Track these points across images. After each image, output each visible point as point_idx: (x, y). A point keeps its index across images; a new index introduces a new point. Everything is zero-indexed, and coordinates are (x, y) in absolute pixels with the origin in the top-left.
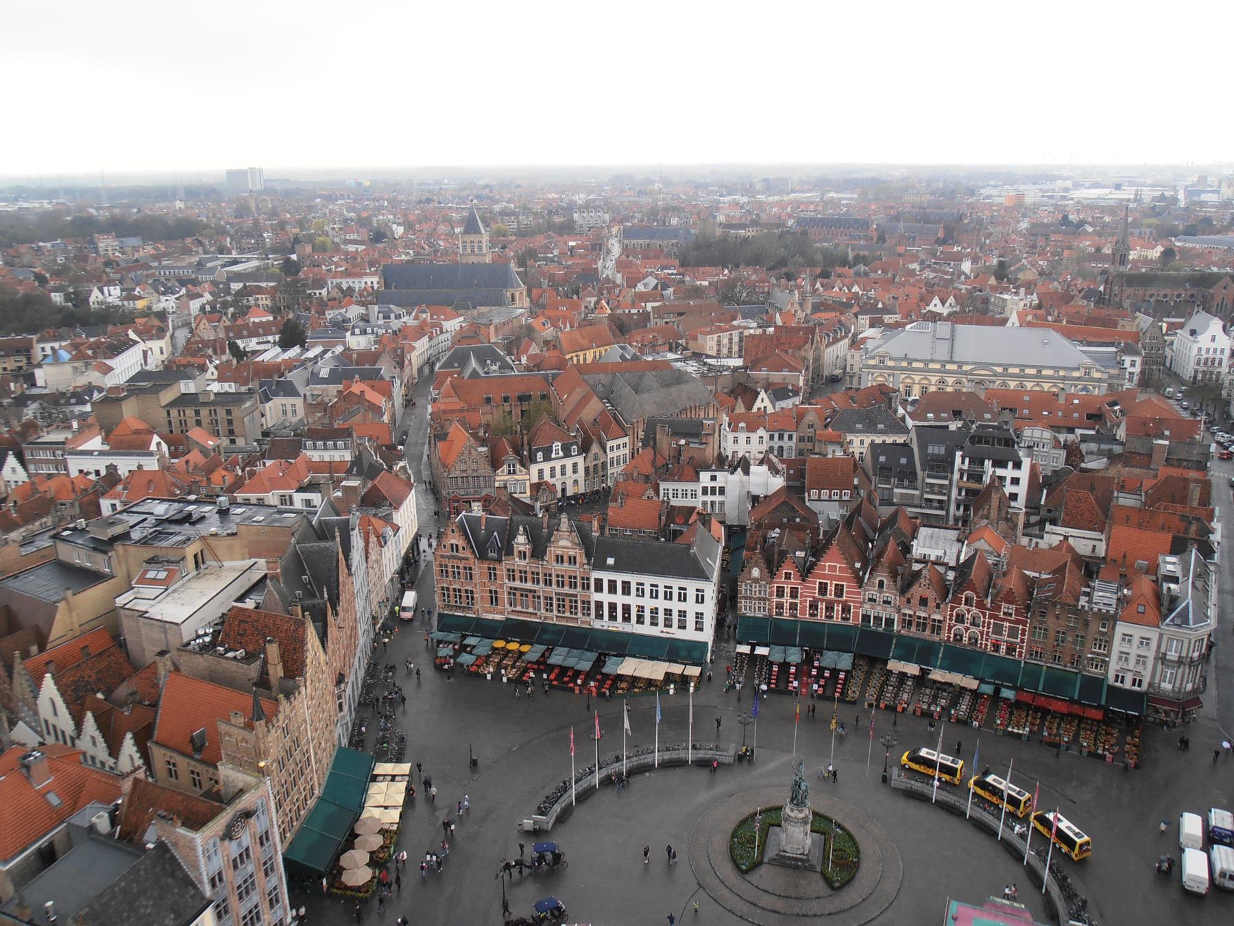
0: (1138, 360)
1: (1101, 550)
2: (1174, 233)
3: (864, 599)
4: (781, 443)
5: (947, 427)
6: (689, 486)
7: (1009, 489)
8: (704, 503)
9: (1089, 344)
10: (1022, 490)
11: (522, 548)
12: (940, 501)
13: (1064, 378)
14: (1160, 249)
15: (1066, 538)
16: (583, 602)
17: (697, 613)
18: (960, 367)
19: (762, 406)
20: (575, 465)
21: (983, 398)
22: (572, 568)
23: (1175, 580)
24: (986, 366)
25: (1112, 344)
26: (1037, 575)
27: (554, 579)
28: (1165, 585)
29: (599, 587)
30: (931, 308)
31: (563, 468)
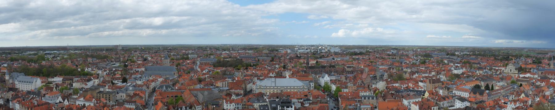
4: (238, 106)
19: (233, 98)
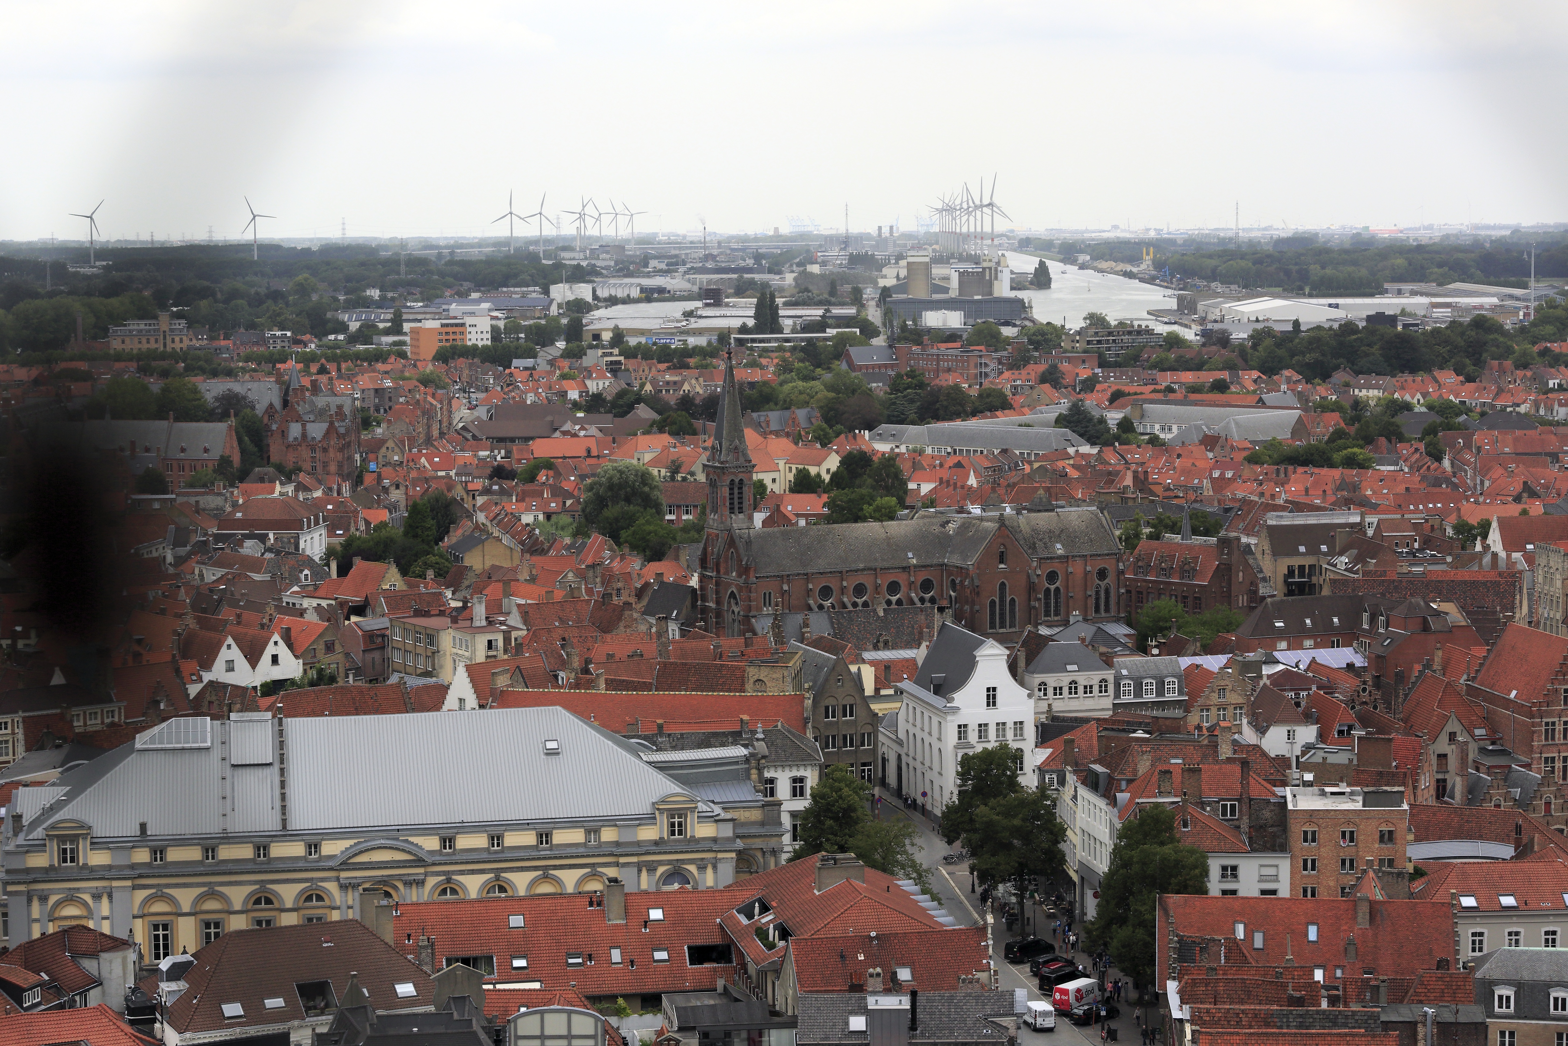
0: (811, 778)
9: (679, 743)
13: (617, 851)
18: (313, 847)
21: (389, 938)
25: (735, 738)
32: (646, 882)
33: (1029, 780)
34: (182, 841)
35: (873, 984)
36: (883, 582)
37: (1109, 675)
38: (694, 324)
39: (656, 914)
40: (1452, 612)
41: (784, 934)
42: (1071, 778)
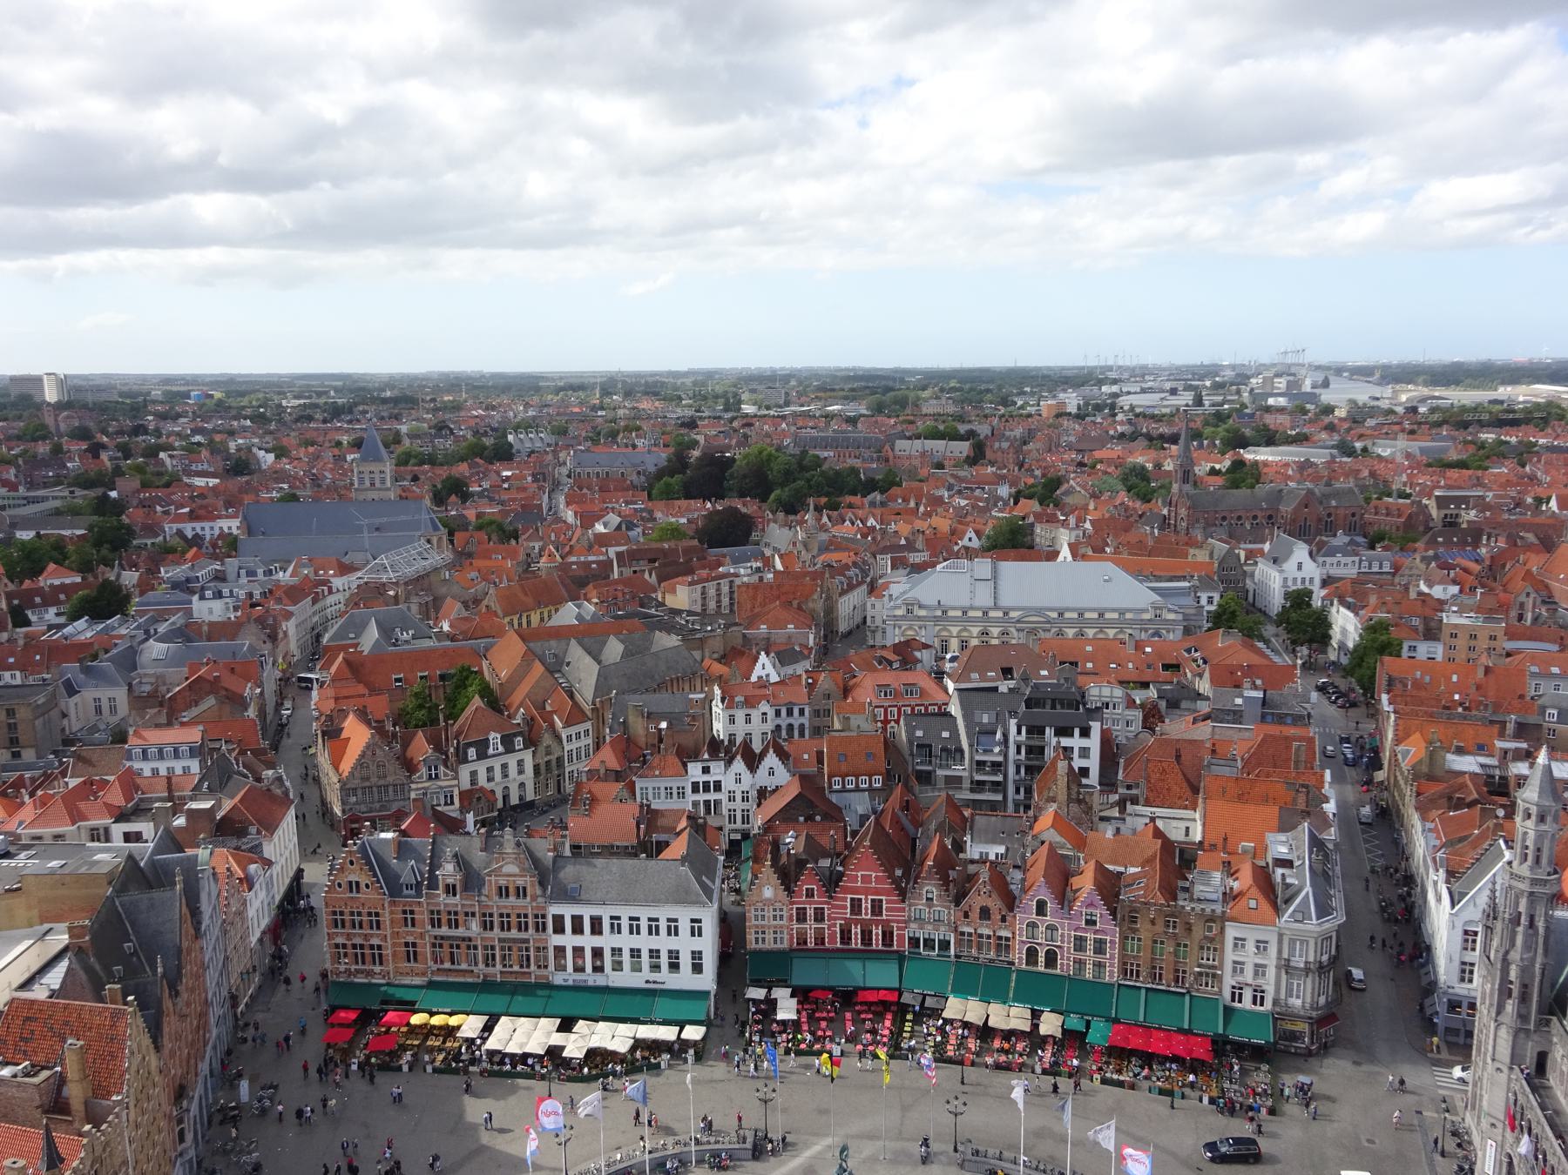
1: (1197, 835)
2: (1244, 443)
3: (909, 916)
4: (790, 720)
5: (996, 689)
6: (674, 783)
7: (1078, 763)
8: (695, 804)
9: (1159, 579)
10: (1093, 763)
11: (450, 881)
12: (998, 783)
14: (1227, 463)
15: (1153, 820)
16: (538, 949)
17: (693, 952)
18: (1006, 614)
19: (763, 674)
20: (520, 763)
22: (521, 902)
23: (1287, 864)
24: (1039, 611)
25: (1183, 578)
26: (1122, 869)
27: (496, 920)
28: (1279, 871)
29: (559, 929)
30: (965, 542)
31: (504, 767)
32: (1143, 636)
33: (1317, 603)
34: (954, 608)
35: (1247, 685)
36: (1251, 515)
37: (1357, 559)
38: (1165, 403)
39: (1148, 650)
40: (1530, 537)
41: (1205, 662)
42: (1335, 602)
